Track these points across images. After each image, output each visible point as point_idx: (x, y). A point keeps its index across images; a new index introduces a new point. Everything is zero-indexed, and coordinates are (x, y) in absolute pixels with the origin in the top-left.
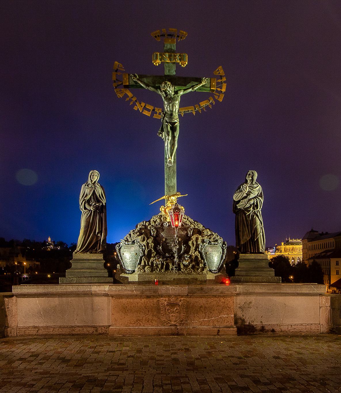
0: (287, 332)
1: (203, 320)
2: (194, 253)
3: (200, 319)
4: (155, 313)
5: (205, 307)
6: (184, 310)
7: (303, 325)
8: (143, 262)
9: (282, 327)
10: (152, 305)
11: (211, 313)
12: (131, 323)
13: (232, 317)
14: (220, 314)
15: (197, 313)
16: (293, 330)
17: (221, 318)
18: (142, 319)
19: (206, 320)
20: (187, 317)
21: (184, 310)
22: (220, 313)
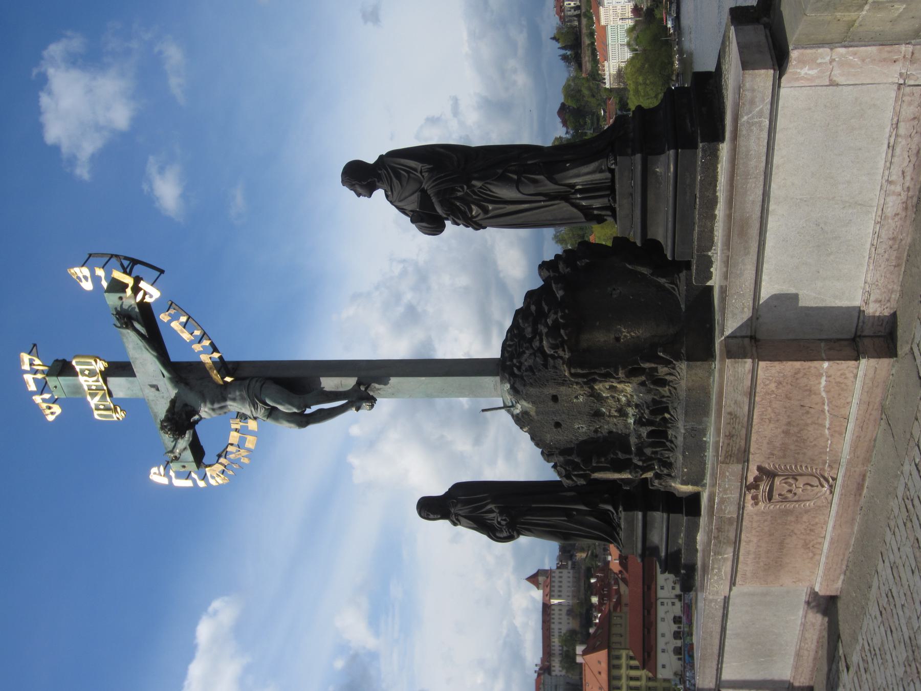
0: (912, 197)
1: (829, 429)
3: (822, 435)
4: (791, 518)
5: (789, 424)
6: (791, 467)
7: (892, 144)
9: (889, 211)
10: (766, 523)
11: (808, 413)
12: (812, 558)
13: (830, 367)
14: (815, 394)
15: (804, 441)
16: (908, 178)
17: (828, 392)
18: (805, 540)
19: (827, 424)
20: (813, 460)
21: (791, 467)
22: (810, 391)
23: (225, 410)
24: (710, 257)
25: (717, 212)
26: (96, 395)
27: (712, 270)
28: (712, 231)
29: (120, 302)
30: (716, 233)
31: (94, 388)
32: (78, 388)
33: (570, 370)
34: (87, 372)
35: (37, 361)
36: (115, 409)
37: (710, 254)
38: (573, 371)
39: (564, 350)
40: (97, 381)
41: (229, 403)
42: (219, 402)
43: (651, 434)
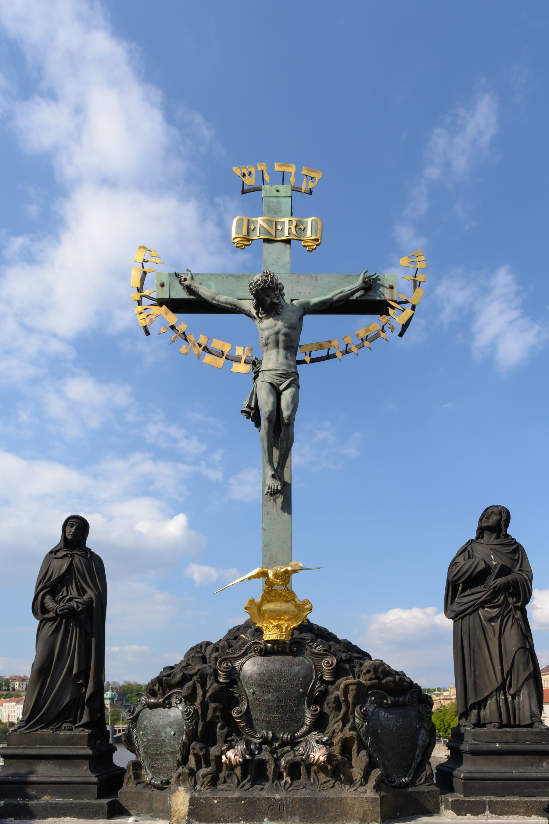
2: (342, 730)
8: (192, 758)
23: (271, 345)
24: (483, 812)
25: (533, 817)
26: (271, 227)
27: (468, 815)
28: (514, 813)
29: (387, 285)
30: (511, 816)
31: (279, 228)
32: (277, 212)
33: (354, 684)
34: (301, 227)
35: (311, 185)
36: (249, 240)
37: (487, 812)
38: (351, 688)
39: (371, 679)
40: (289, 234)
41: (282, 352)
42: (285, 341)
43: (263, 763)
